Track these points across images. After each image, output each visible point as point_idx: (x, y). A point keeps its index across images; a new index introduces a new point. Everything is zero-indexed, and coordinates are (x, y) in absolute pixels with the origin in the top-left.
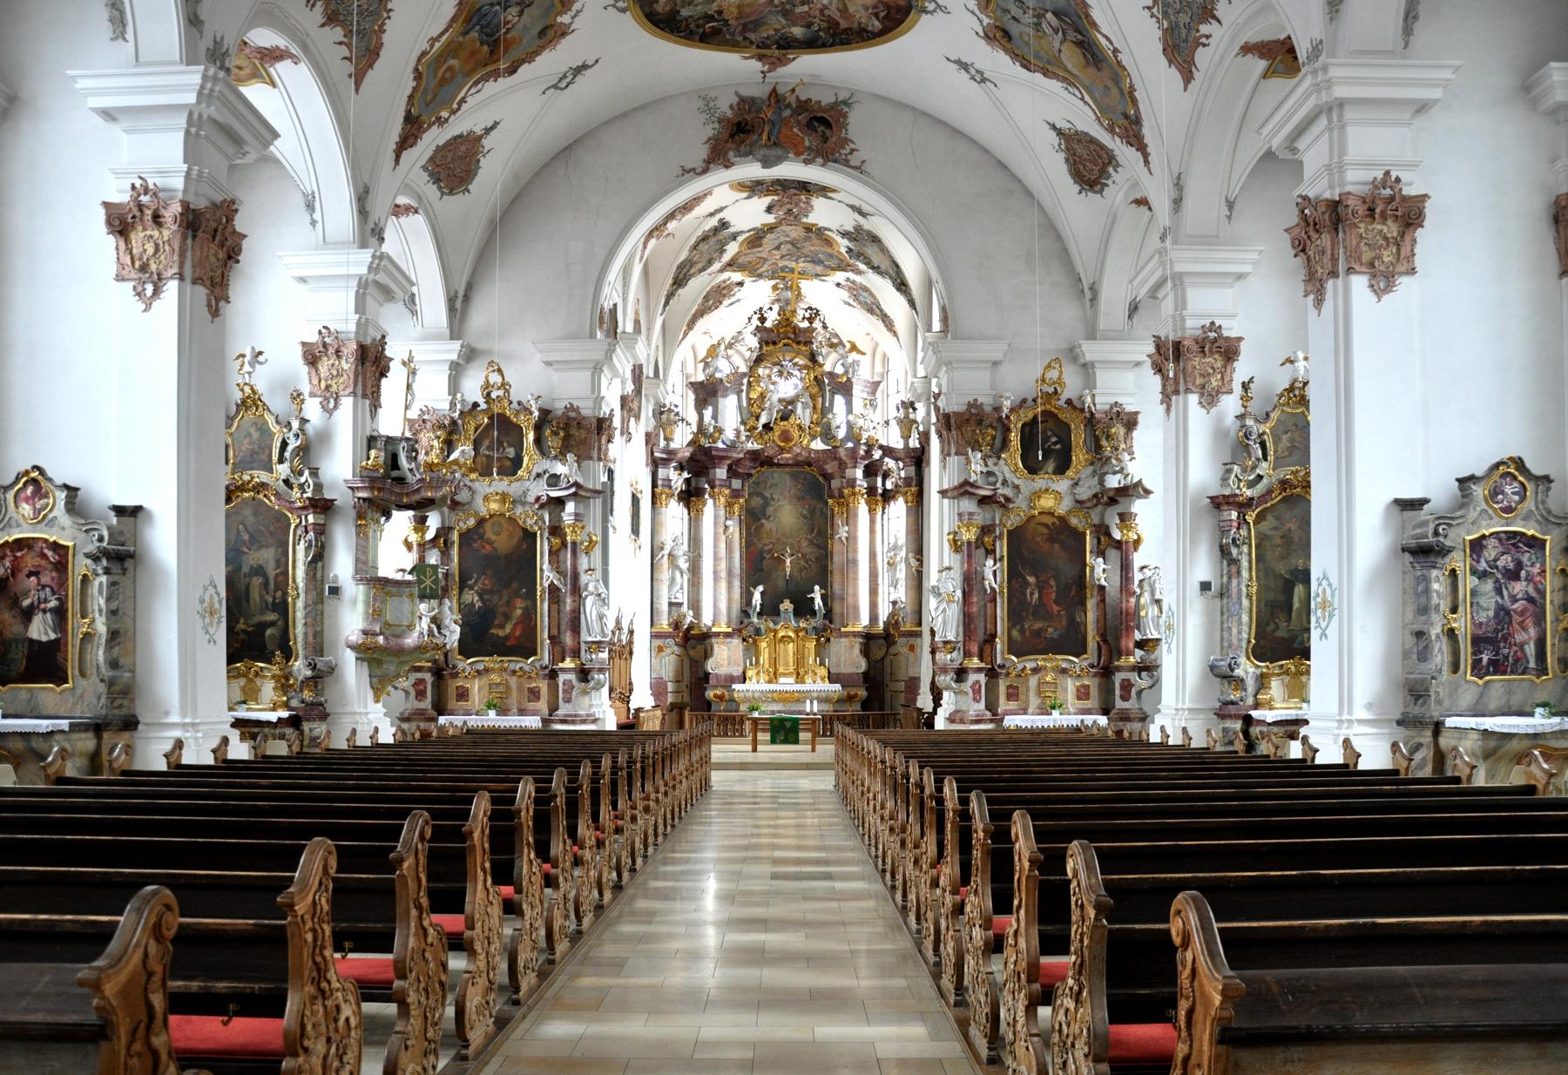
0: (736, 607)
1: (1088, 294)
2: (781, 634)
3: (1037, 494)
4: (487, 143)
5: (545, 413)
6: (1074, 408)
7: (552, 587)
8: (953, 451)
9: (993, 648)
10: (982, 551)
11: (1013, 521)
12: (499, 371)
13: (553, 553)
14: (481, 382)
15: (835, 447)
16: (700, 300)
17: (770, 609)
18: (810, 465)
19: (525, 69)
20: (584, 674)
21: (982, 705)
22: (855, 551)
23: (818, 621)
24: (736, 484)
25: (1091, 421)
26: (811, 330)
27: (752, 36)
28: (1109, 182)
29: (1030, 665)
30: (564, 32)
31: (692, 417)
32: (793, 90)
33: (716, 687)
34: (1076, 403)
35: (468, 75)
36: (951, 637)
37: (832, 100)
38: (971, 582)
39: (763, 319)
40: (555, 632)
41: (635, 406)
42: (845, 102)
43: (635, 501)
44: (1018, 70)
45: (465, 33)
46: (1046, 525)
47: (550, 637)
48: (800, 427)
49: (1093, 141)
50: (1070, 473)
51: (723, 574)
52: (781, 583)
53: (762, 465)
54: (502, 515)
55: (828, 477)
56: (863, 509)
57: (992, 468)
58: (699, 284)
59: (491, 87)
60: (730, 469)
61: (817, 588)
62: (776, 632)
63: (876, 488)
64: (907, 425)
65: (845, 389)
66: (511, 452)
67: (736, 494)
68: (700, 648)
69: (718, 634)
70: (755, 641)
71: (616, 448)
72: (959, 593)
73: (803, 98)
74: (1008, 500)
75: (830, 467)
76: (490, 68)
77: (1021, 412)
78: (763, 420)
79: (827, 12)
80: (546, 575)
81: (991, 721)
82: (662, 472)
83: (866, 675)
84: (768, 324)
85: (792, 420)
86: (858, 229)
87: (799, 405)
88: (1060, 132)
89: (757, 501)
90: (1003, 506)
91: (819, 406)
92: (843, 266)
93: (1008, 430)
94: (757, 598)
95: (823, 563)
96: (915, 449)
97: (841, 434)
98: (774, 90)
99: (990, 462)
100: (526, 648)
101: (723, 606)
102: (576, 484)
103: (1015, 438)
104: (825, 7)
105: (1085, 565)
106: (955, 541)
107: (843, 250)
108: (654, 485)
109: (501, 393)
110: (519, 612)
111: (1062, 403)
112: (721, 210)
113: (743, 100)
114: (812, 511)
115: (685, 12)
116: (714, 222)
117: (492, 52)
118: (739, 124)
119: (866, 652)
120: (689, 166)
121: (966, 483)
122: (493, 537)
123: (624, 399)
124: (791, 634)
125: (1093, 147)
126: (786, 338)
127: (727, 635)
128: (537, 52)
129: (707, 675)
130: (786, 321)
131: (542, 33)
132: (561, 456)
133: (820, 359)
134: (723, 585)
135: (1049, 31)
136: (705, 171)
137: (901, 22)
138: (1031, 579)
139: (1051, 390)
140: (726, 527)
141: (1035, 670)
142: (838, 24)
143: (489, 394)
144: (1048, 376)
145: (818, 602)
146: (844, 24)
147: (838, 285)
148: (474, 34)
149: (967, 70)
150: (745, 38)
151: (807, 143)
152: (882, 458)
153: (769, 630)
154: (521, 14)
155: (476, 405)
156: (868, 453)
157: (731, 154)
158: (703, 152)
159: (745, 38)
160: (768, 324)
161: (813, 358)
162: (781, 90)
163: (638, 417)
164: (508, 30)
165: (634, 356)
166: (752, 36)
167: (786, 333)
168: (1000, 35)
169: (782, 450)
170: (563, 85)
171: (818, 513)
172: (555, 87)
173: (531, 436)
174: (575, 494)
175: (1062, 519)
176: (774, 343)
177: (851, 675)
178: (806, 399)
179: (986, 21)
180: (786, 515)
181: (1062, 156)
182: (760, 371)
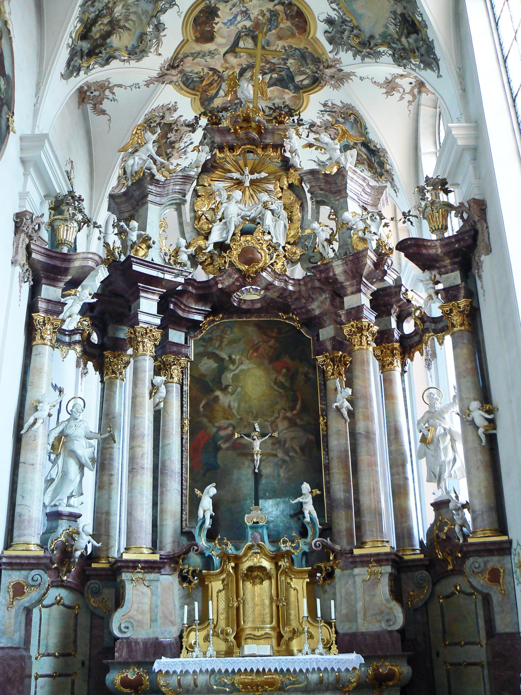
18: (286, 309)
22: (369, 418)
24: (176, 336)
33: (125, 665)
51: (148, 462)
55: (313, 323)
56: (373, 366)
60: (162, 308)
62: (237, 559)
69: (132, 565)
70: (202, 580)
75: (317, 306)
78: (215, 237)
85: (258, 234)
89: (208, 365)
92: (316, 82)
94: (206, 505)
95: (311, 441)
108: (32, 308)
114: (292, 377)
119: (397, 593)
124: (266, 564)
127: (151, 567)
129: (116, 639)
134: (146, 480)
140: (154, 389)
153: (225, 557)
169: (244, 279)
171: (301, 378)
176: (232, 149)
177: (377, 636)
180: (252, 382)
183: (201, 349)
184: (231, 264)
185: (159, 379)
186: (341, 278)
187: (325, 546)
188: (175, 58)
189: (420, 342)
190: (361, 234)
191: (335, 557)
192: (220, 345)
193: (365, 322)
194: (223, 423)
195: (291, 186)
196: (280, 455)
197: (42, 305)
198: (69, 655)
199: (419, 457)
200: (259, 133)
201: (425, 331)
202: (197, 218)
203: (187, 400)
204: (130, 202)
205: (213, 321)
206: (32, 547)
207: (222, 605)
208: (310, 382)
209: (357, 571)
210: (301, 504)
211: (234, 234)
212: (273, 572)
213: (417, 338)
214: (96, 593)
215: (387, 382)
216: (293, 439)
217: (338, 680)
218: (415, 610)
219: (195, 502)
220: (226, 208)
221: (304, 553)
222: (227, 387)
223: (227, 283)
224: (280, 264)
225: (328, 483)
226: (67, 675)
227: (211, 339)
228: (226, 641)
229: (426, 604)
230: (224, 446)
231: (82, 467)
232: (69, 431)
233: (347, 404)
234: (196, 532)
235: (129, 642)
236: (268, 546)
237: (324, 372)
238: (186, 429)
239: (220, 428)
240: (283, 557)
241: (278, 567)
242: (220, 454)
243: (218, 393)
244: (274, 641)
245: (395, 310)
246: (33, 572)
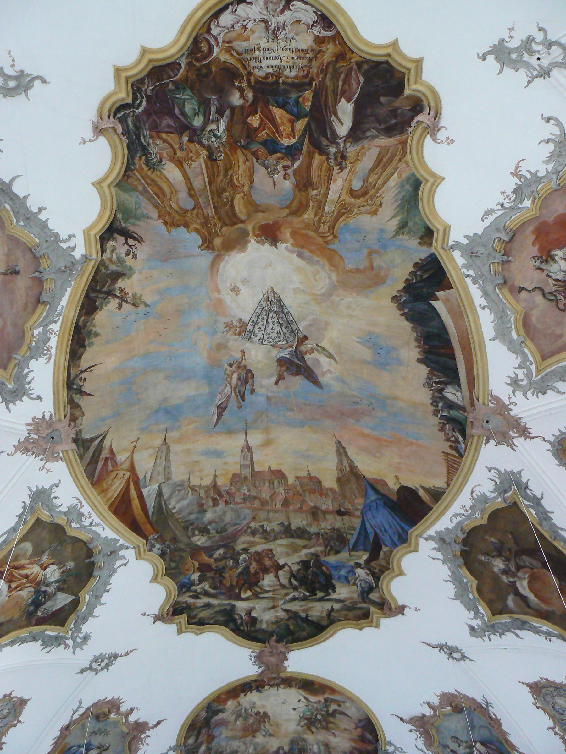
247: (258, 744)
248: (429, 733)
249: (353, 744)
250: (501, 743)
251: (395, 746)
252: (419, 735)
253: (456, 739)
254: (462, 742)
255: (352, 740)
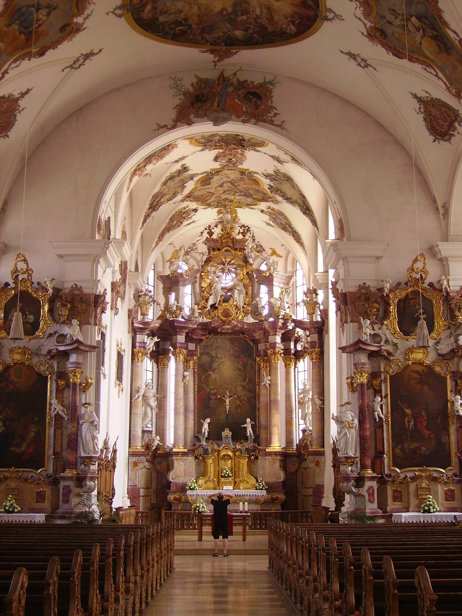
0: (190, 433)
1: (441, 211)
2: (223, 453)
3: (411, 350)
4: (22, 103)
5: (57, 290)
6: (435, 289)
7: (58, 417)
8: (349, 319)
9: (382, 462)
10: (371, 391)
11: (393, 369)
12: (25, 260)
13: (59, 391)
14: (11, 268)
15: (262, 321)
16: (167, 221)
17: (215, 435)
18: (243, 333)
19: (50, 54)
20: (80, 481)
21: (375, 505)
22: (276, 393)
23: (249, 444)
24: (192, 346)
25: (447, 298)
26: (244, 241)
27: (207, 37)
28: (455, 133)
29: (409, 475)
30: (78, 29)
31: (161, 300)
32: (235, 74)
33: (175, 492)
34: (436, 285)
35: (10, 54)
36: (351, 454)
37: (262, 81)
38: (364, 413)
39: (211, 233)
40: (58, 449)
41: (121, 289)
42: (270, 83)
43: (120, 357)
44: (390, 57)
45: (9, 25)
46: (417, 372)
47: (54, 454)
48: (237, 307)
49: (444, 105)
50: (434, 335)
51: (182, 410)
52: (223, 417)
53: (209, 333)
54: (23, 363)
55: (256, 342)
57: (377, 331)
58: (167, 209)
59: (26, 64)
61: (248, 420)
62: (219, 452)
63: (290, 349)
64: (311, 305)
65: (268, 281)
66: (31, 318)
67: (191, 354)
68: (164, 463)
69: (177, 454)
70: (204, 459)
71: (106, 318)
72: (356, 421)
73: (242, 79)
74: (390, 354)
75: (258, 335)
76: (26, 51)
77: (397, 292)
78: (211, 302)
79: (259, 21)
80: (54, 406)
81: (382, 517)
82: (139, 338)
83: (284, 483)
84: (214, 237)
85: (231, 302)
86: (277, 172)
87: (236, 292)
88: (420, 100)
90: (386, 358)
91: (250, 292)
92: (265, 198)
93: (389, 305)
94: (206, 426)
96: (317, 322)
97: (265, 312)
98: (222, 74)
99: (376, 327)
100: (38, 462)
101: (181, 433)
102: (78, 341)
103: (393, 309)
104: (258, 17)
105: (447, 401)
106: (352, 384)
107: (266, 187)
108: (134, 346)
109: (25, 276)
110: (32, 434)
111: (426, 285)
112: (183, 158)
113: (200, 80)
114: (245, 366)
115: (162, 19)
116: (178, 167)
117: (27, 40)
118: (197, 96)
119: (284, 466)
120: (162, 124)
121: (359, 342)
122: (15, 380)
123: (113, 284)
124: (230, 453)
125: (443, 109)
126: (226, 246)
127: (184, 454)
128: (60, 41)
130: (227, 235)
131: (63, 29)
132: (68, 322)
133: (251, 261)
134: (181, 418)
135: (413, 29)
136: (174, 127)
137: (310, 27)
138: (408, 411)
139: (418, 276)
140: (184, 377)
141: (414, 479)
142: (266, 29)
143: (17, 277)
144: (416, 266)
145: (249, 430)
146: (270, 29)
147: (262, 211)
148: (15, 26)
149: (355, 60)
150: (203, 38)
151: (244, 109)
152: (294, 328)
153: (214, 450)
154: (48, 14)
155: (7, 284)
156: (285, 324)
157: (192, 116)
158: (172, 115)
159: (203, 38)
160: (214, 237)
161: (245, 260)
162: (226, 74)
163: (123, 298)
164: (40, 25)
165: (122, 255)
166: (207, 37)
167: (227, 243)
168: (378, 34)
170: (77, 66)
172: (71, 67)
173: (46, 308)
174: (77, 349)
175: (429, 367)
176: (219, 250)
178: (241, 287)
179: (369, 24)
180: (226, 368)
181: (421, 117)
182: (209, 268)
183: (202, 351)
184: (218, 316)
185: (186, 373)
186: (268, 328)
187: (254, 447)
188: (190, 193)
189: (303, 356)
190: (277, 309)
191: (259, 452)
192: (212, 349)
193: (277, 350)
194: (213, 387)
195: (247, 273)
196: (238, 402)
197: (137, 344)
198: (149, 488)
199: (299, 409)
200: (233, 242)
201: (305, 352)
202: (202, 291)
203: (196, 376)
204: (171, 283)
205: (208, 337)
206: (139, 448)
207: (212, 469)
208: (253, 368)
209: (267, 457)
210: (246, 428)
211: (220, 301)
212: (233, 457)
213: (302, 353)
214: (160, 463)
215: (288, 373)
216: (245, 395)
217: (256, 499)
218: (292, 473)
219: (201, 425)
220: (216, 286)
221: (246, 449)
222: (215, 369)
223: (216, 325)
224: (241, 316)
225: (259, 416)
226: (148, 496)
227: (207, 346)
228: (214, 483)
229: (296, 471)
230: (213, 398)
231: (152, 409)
232: (147, 395)
233: (269, 382)
234: (201, 437)
235: (176, 484)
236: (232, 446)
237: (259, 365)
238: (196, 389)
239: (211, 389)
240: (237, 451)
241: (235, 455)
242: (211, 401)
243: (210, 372)
244: (233, 484)
245: (293, 339)
246: (141, 457)
247: (202, 5)
248: (368, 4)
249: (295, 9)
250: (435, 19)
251: (334, 13)
252: (359, 5)
253: (393, 11)
254: (399, 14)
255: (294, 5)
